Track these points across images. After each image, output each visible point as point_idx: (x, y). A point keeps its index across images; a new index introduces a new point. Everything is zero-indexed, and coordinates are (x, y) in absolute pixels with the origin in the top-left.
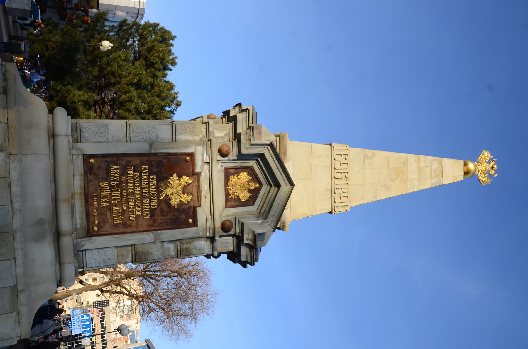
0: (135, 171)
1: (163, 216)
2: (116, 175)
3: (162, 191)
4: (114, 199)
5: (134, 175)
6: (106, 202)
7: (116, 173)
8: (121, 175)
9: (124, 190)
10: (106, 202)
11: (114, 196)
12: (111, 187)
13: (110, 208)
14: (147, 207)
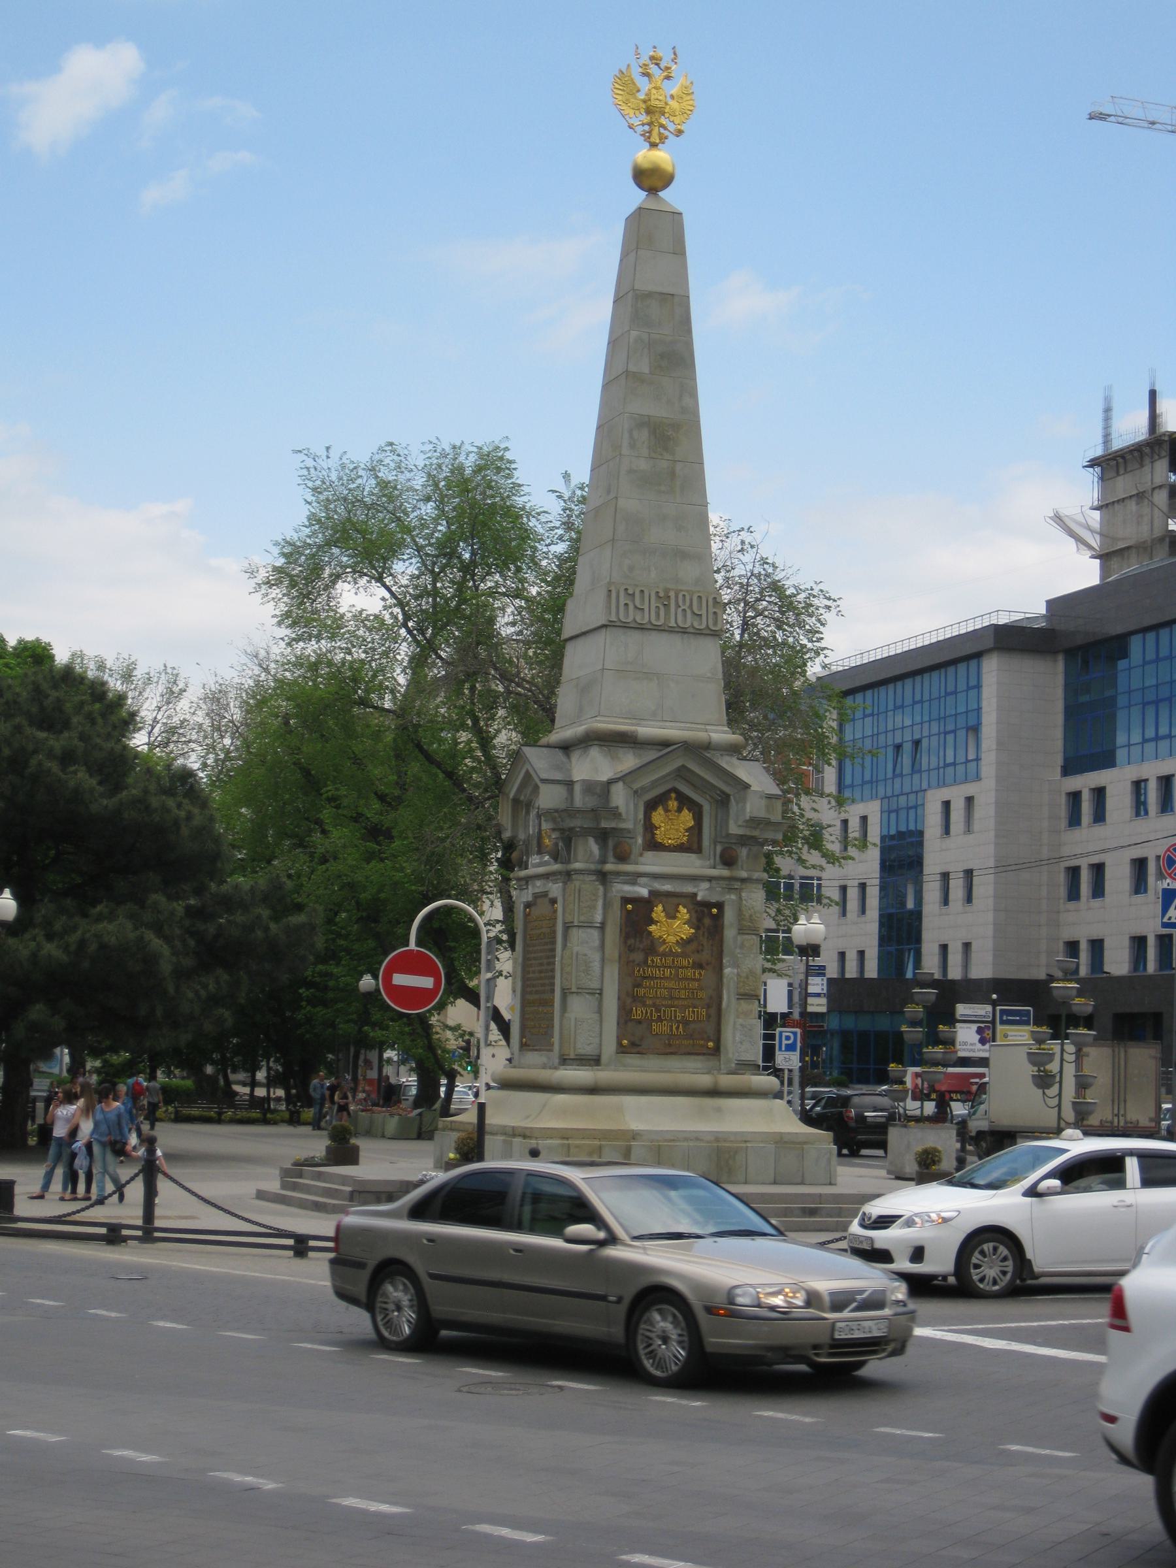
0: (639, 985)
1: (702, 950)
2: (644, 1012)
3: (671, 950)
4: (675, 1017)
5: (645, 988)
6: (678, 1028)
7: (642, 1012)
8: (644, 1005)
9: (663, 1003)
10: (678, 1028)
11: (671, 1018)
12: (660, 1019)
13: (686, 1023)
14: (689, 973)
